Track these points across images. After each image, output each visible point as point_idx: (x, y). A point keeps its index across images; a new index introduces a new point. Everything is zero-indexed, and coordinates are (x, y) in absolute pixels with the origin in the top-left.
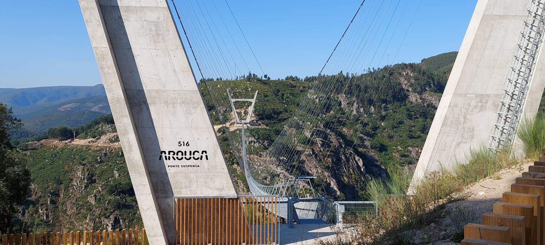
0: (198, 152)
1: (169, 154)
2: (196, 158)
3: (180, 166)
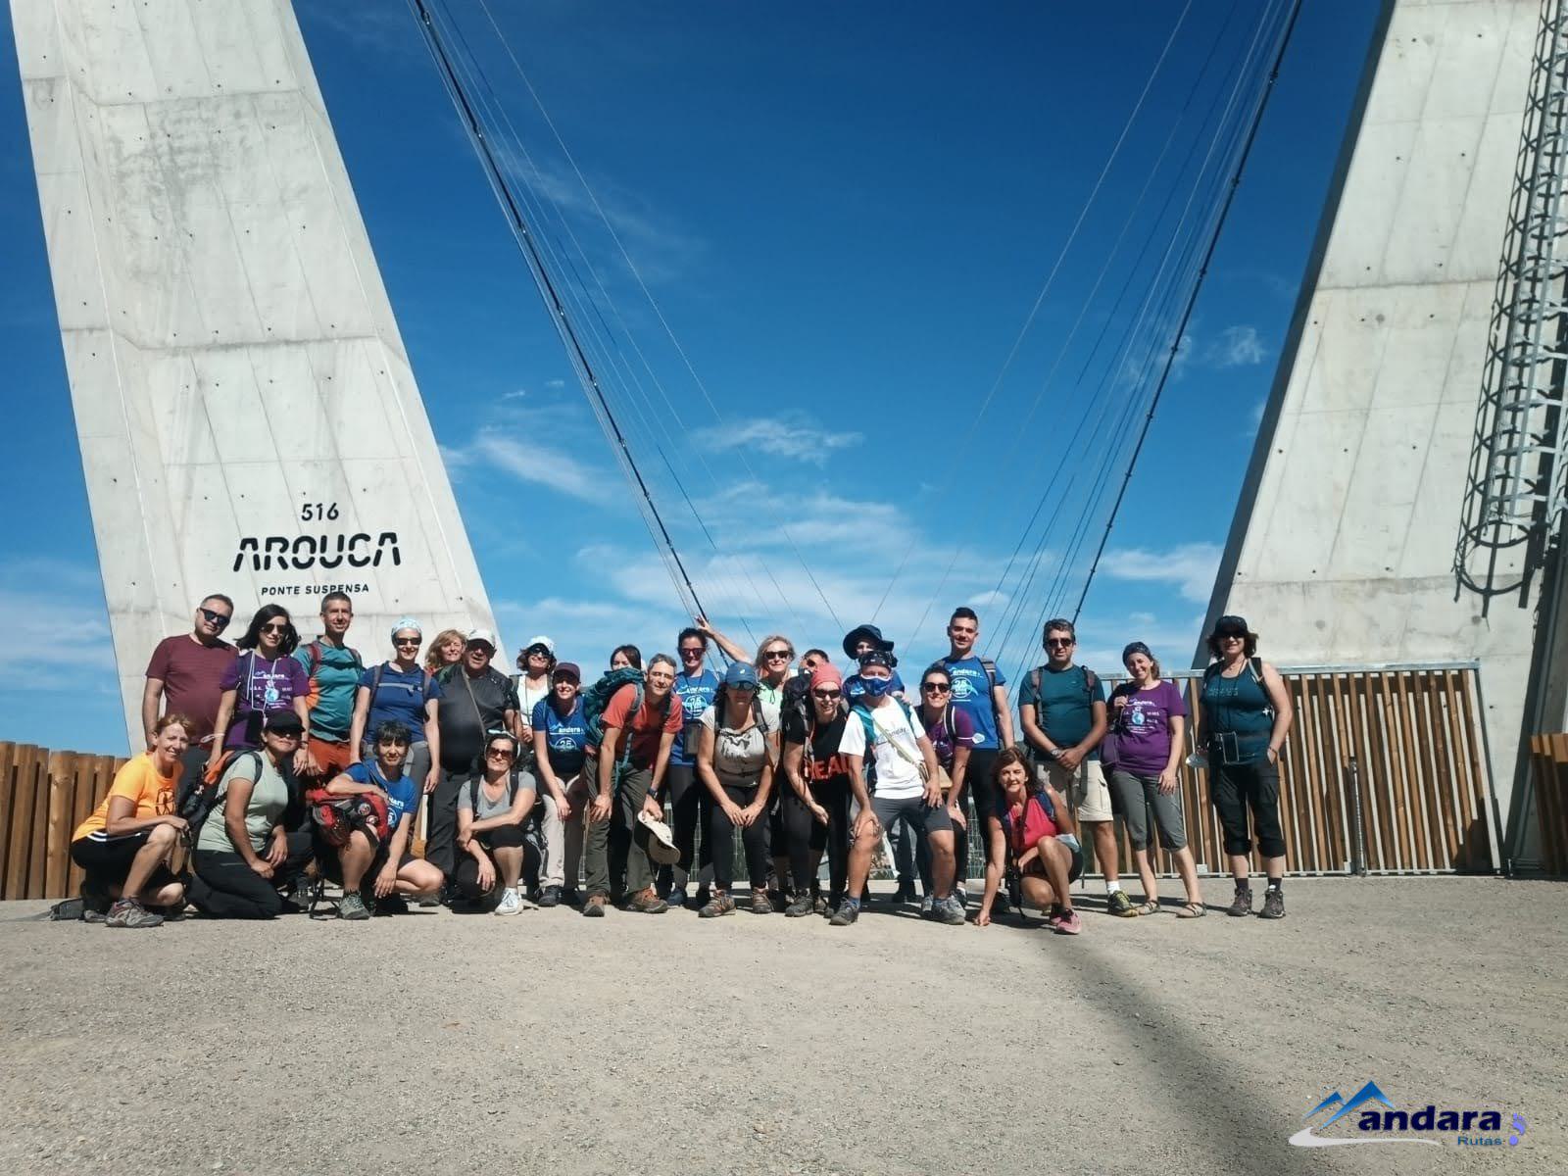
0: (367, 538)
1: (268, 548)
2: (359, 558)
3: (303, 590)
